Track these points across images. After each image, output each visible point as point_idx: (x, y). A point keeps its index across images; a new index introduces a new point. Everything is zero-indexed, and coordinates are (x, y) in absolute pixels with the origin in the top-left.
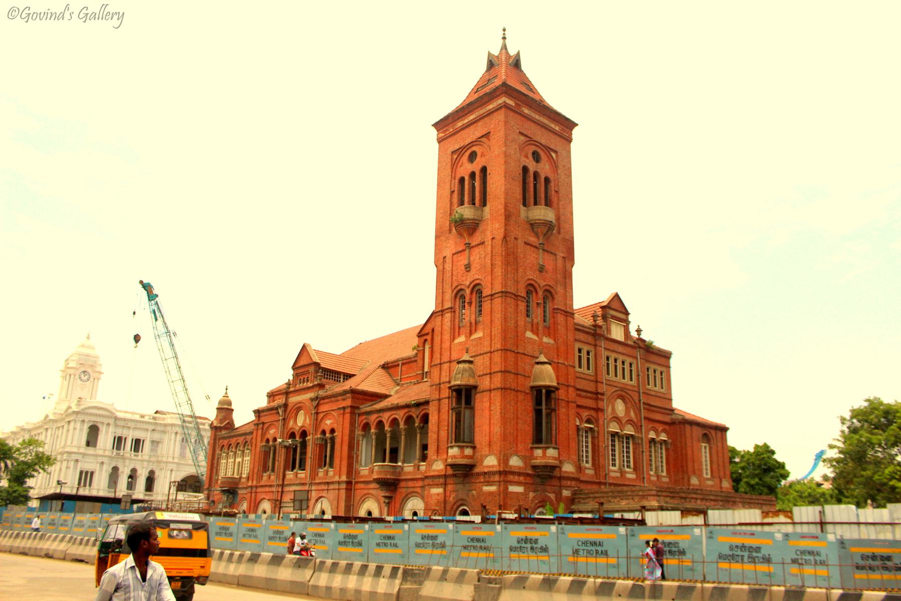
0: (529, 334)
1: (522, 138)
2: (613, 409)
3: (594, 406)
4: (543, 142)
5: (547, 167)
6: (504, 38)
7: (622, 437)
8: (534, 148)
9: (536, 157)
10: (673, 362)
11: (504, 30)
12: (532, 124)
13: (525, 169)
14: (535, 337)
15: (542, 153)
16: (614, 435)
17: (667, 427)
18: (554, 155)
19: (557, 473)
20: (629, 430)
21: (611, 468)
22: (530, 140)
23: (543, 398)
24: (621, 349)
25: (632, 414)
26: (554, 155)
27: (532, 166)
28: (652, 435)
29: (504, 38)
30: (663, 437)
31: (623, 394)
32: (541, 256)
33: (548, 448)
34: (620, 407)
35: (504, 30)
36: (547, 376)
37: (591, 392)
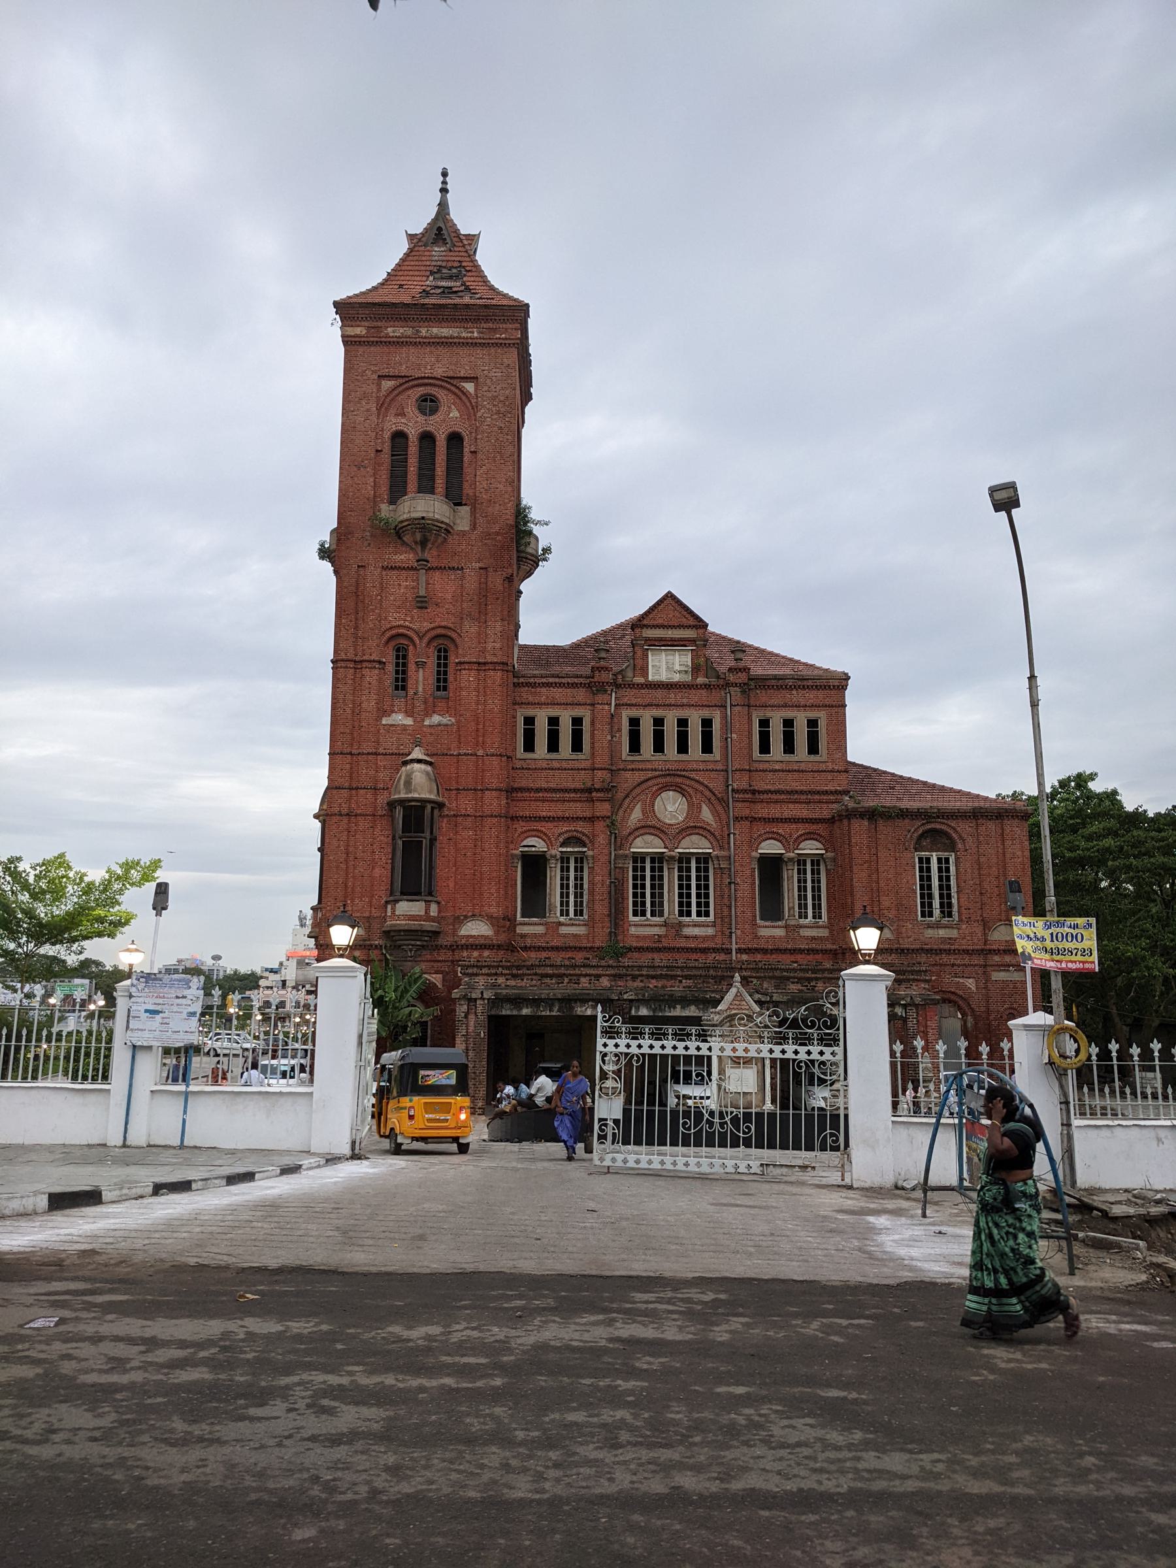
0: (399, 718)
1: (387, 384)
2: (649, 809)
3: (588, 814)
4: (439, 372)
5: (455, 414)
6: (444, 191)
7: (672, 858)
8: (422, 390)
9: (428, 405)
10: (850, 695)
11: (445, 174)
12: (412, 350)
13: (399, 437)
14: (409, 721)
15: (441, 394)
16: (658, 859)
17: (820, 828)
18: (470, 387)
19: (442, 941)
20: (696, 845)
21: (631, 918)
22: (406, 381)
23: (415, 817)
24: (672, 697)
25: (706, 814)
26: (470, 387)
27: (413, 424)
28: (771, 848)
29: (444, 191)
30: (811, 848)
31: (674, 780)
32: (423, 579)
33: (397, 901)
34: (671, 807)
35: (445, 174)
36: (419, 781)
37: (575, 791)
